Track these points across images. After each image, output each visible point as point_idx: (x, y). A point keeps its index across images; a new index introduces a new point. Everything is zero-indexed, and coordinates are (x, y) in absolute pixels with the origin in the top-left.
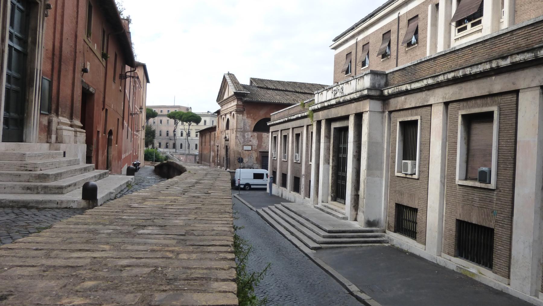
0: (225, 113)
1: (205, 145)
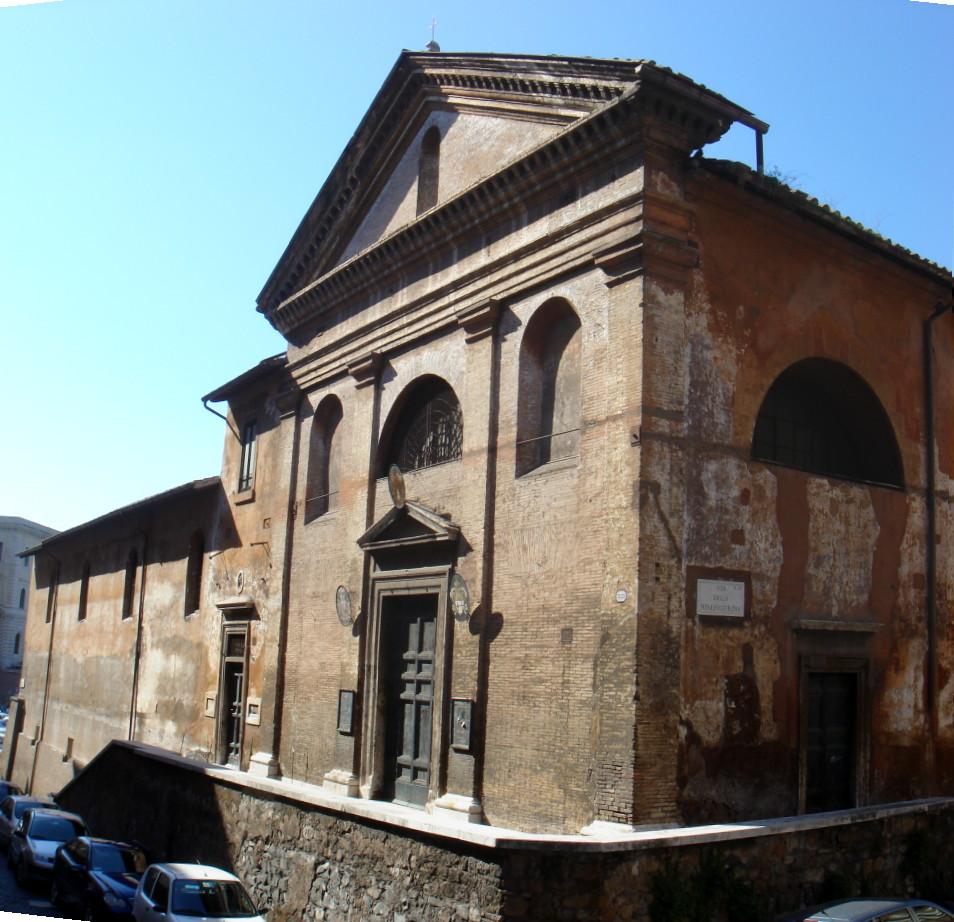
0: (381, 346)
1: (82, 615)
